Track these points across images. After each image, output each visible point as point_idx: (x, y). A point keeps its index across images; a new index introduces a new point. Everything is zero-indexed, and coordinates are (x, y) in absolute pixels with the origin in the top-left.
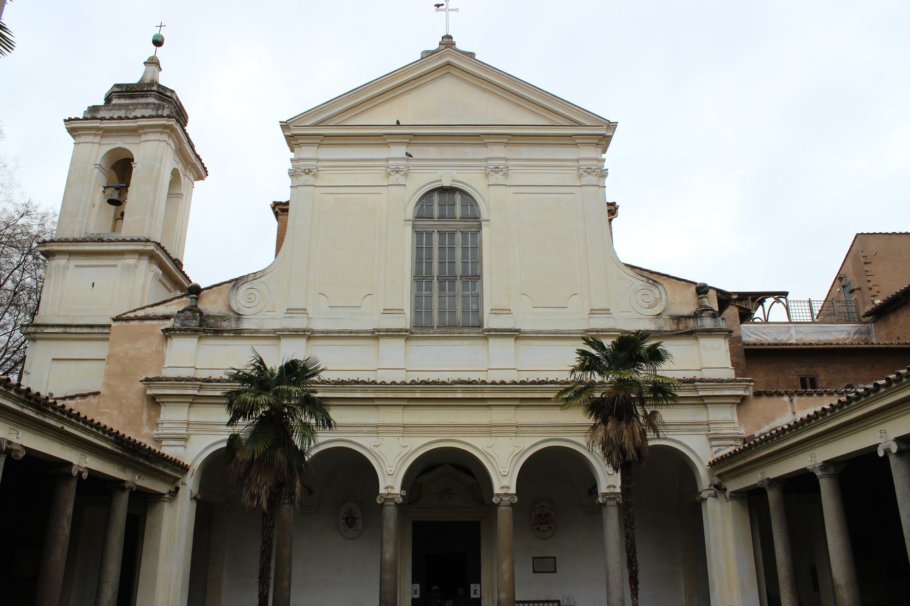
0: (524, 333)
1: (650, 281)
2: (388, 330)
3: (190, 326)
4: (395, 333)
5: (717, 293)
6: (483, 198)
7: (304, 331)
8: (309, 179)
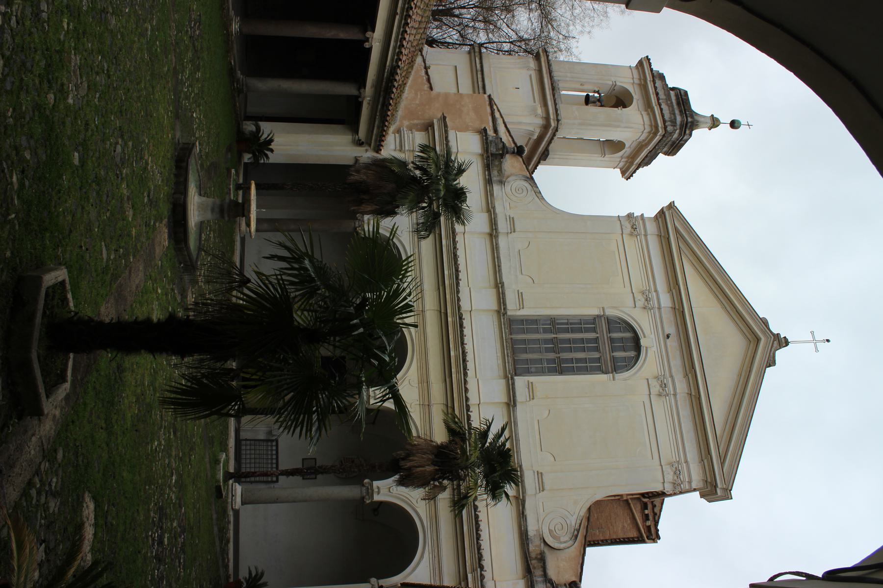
0: (513, 410)
1: (576, 532)
2: (504, 294)
3: (491, 147)
4: (501, 300)
6: (636, 373)
7: (496, 229)
8: (628, 229)
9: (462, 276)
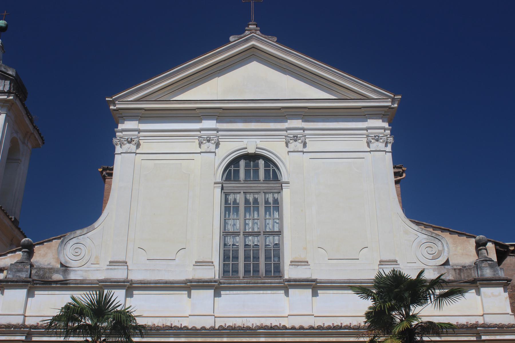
5: (495, 245)
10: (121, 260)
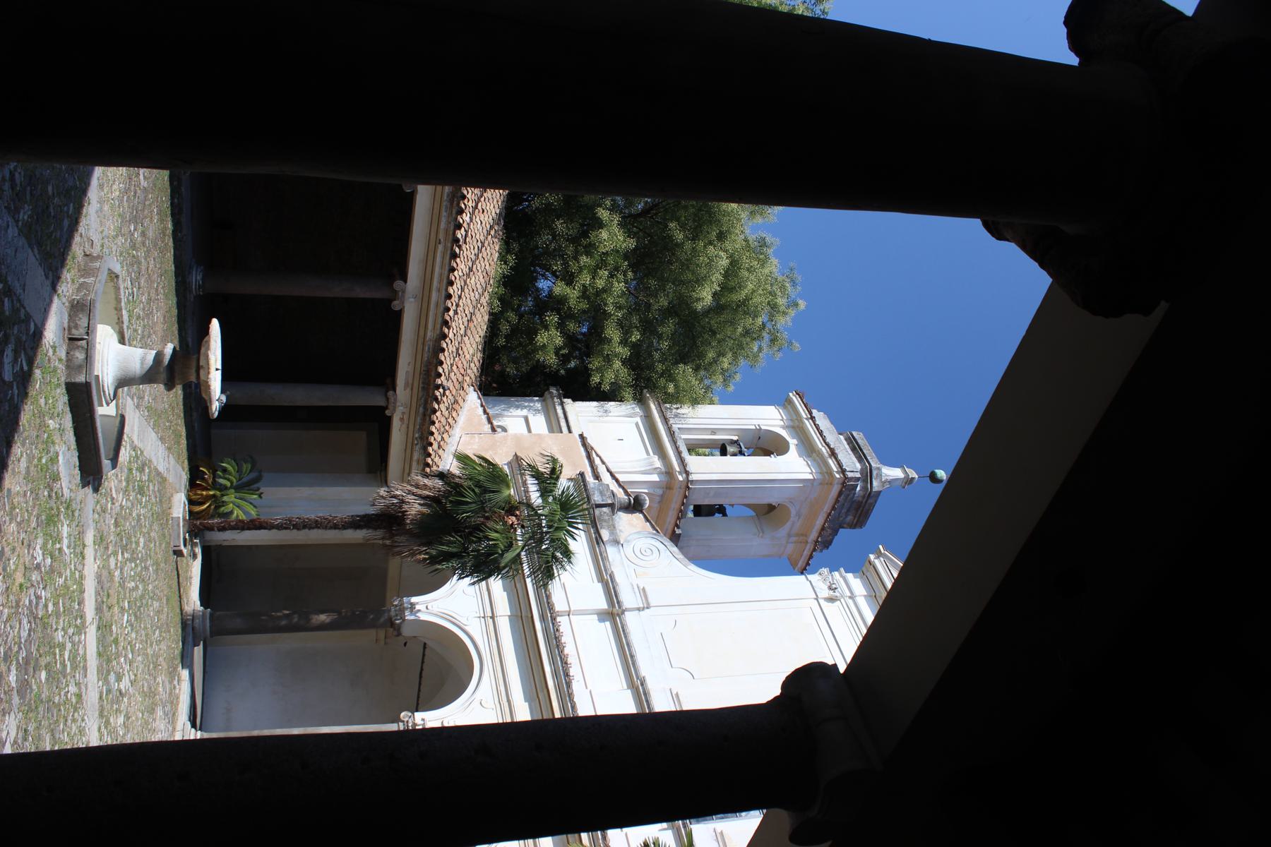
9: (574, 671)
10: (650, 600)
